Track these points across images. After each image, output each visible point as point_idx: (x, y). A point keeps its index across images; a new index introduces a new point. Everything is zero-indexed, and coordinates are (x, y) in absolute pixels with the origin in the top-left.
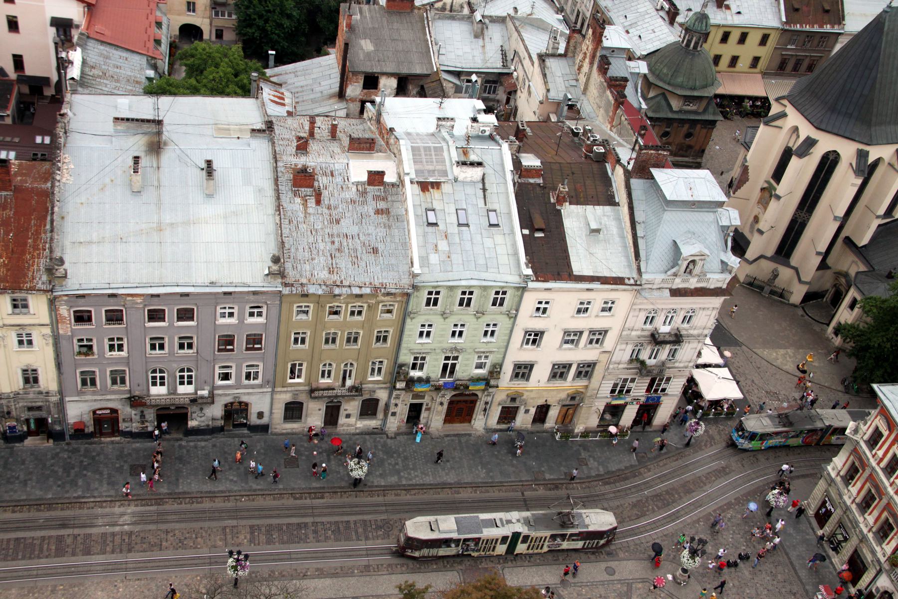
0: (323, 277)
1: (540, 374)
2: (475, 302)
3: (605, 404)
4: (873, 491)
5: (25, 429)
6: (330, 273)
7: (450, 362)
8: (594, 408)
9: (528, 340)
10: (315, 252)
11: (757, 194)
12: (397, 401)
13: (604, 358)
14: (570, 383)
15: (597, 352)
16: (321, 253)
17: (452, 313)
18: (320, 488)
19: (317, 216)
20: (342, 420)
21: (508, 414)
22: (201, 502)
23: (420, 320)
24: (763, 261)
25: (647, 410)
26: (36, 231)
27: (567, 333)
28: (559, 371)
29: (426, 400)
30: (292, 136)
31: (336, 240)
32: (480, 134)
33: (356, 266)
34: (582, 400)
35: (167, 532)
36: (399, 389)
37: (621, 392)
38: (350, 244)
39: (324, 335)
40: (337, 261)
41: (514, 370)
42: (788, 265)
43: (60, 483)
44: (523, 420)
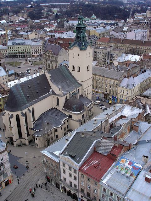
11: (9, 129)
42: (23, 138)
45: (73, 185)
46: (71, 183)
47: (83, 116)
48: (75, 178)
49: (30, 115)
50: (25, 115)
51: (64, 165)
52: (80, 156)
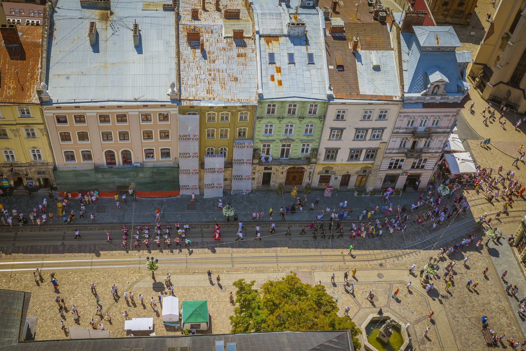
0: (203, 95)
1: (343, 157)
2: (298, 111)
3: (385, 175)
5: (38, 184)
6: (207, 93)
7: (286, 148)
9: (334, 135)
10: (198, 80)
14: (362, 161)
15: (379, 142)
16: (202, 82)
17: (283, 118)
18: (207, 222)
23: (264, 121)
24: (501, 84)
26: (33, 68)
30: (190, 8)
31: (212, 73)
32: (307, 5)
33: (224, 89)
37: (395, 167)
38: (221, 75)
39: (238, 130)
40: (212, 86)
41: (326, 153)
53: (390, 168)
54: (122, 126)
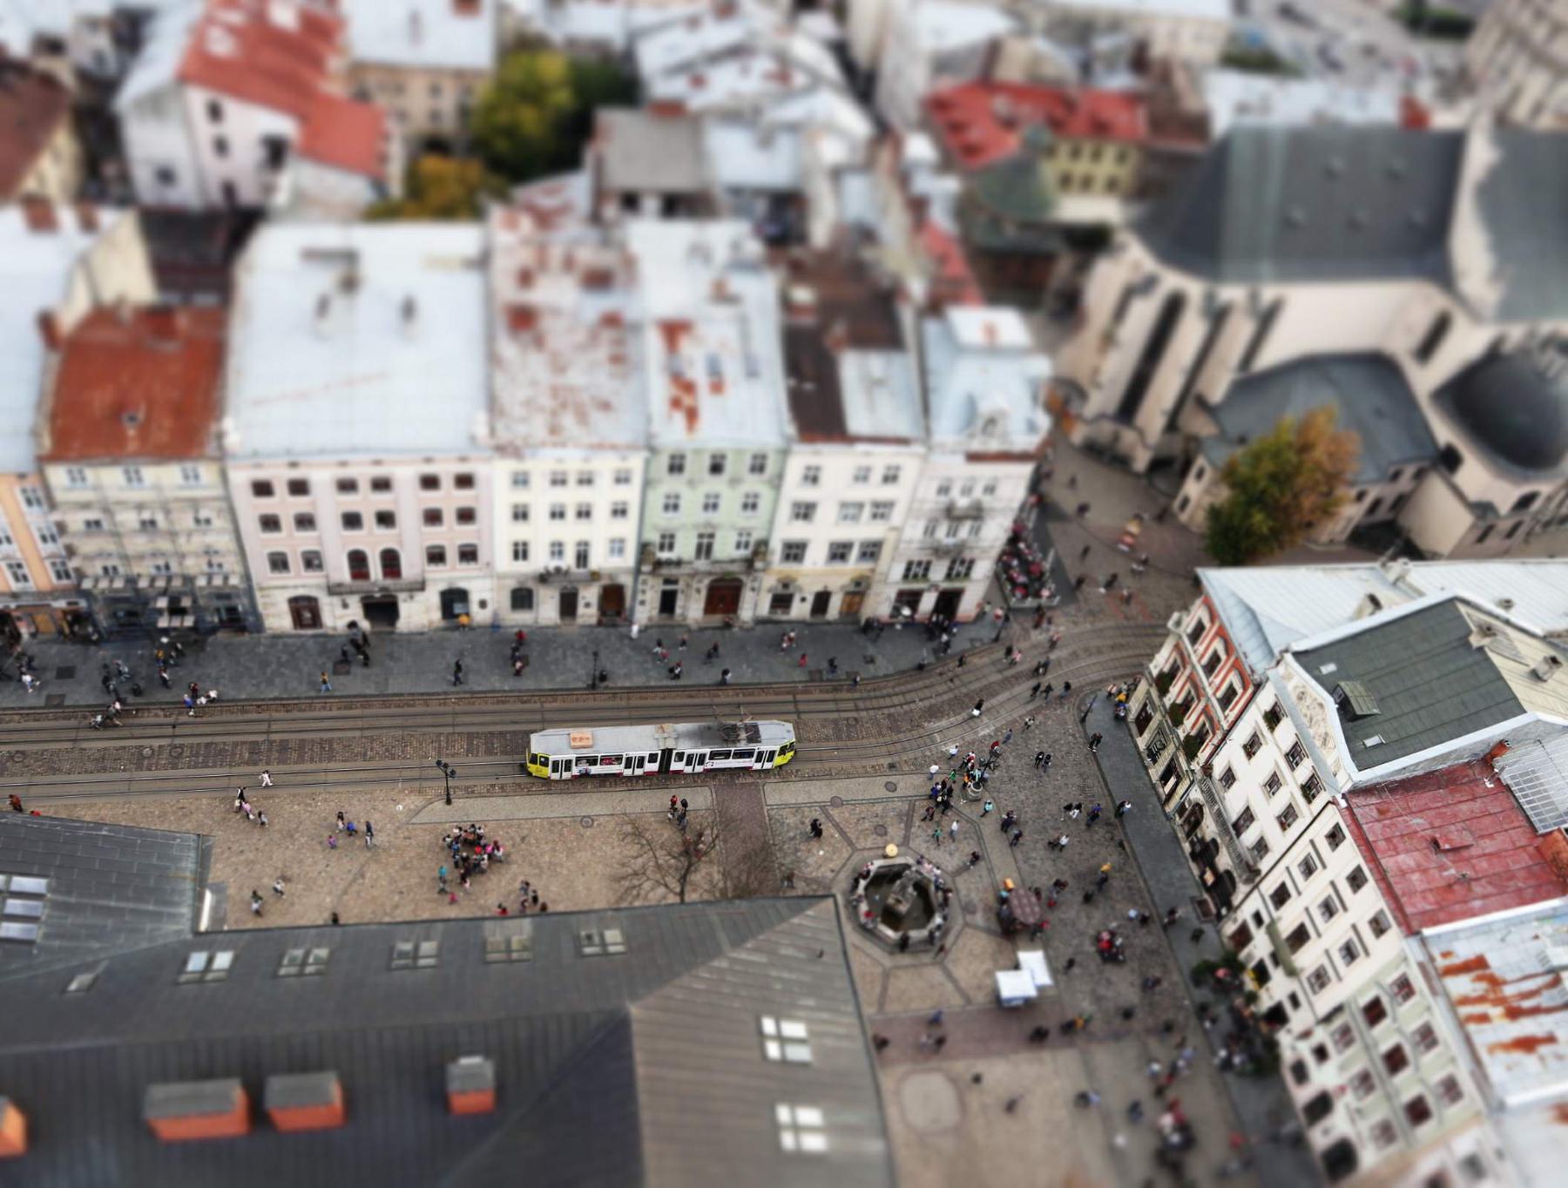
1: (816, 556)
4: (1193, 693)
8: (884, 596)
12: (645, 587)
13: (892, 536)
14: (853, 566)
19: (536, 364)
20: (581, 610)
21: (782, 601)
22: (413, 706)
25: (949, 601)
27: (844, 505)
28: (839, 552)
29: (680, 586)
34: (868, 587)
35: (372, 740)
36: (645, 573)
43: (254, 682)
44: (800, 610)
45: (1249, 837)
46: (1248, 816)
47: (1525, 502)
48: (1286, 818)
49: (1239, 331)
50: (1218, 317)
51: (1273, 718)
52: (1394, 737)
53: (906, 577)
54: (383, 501)
